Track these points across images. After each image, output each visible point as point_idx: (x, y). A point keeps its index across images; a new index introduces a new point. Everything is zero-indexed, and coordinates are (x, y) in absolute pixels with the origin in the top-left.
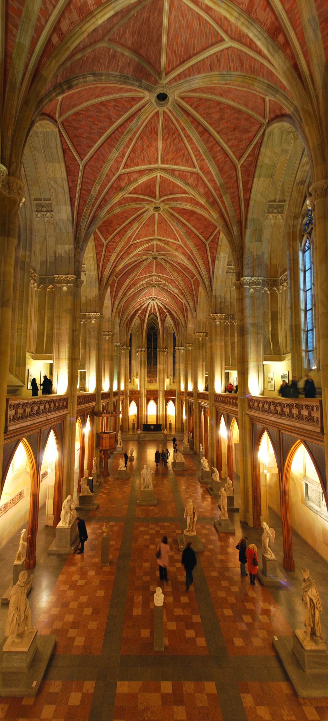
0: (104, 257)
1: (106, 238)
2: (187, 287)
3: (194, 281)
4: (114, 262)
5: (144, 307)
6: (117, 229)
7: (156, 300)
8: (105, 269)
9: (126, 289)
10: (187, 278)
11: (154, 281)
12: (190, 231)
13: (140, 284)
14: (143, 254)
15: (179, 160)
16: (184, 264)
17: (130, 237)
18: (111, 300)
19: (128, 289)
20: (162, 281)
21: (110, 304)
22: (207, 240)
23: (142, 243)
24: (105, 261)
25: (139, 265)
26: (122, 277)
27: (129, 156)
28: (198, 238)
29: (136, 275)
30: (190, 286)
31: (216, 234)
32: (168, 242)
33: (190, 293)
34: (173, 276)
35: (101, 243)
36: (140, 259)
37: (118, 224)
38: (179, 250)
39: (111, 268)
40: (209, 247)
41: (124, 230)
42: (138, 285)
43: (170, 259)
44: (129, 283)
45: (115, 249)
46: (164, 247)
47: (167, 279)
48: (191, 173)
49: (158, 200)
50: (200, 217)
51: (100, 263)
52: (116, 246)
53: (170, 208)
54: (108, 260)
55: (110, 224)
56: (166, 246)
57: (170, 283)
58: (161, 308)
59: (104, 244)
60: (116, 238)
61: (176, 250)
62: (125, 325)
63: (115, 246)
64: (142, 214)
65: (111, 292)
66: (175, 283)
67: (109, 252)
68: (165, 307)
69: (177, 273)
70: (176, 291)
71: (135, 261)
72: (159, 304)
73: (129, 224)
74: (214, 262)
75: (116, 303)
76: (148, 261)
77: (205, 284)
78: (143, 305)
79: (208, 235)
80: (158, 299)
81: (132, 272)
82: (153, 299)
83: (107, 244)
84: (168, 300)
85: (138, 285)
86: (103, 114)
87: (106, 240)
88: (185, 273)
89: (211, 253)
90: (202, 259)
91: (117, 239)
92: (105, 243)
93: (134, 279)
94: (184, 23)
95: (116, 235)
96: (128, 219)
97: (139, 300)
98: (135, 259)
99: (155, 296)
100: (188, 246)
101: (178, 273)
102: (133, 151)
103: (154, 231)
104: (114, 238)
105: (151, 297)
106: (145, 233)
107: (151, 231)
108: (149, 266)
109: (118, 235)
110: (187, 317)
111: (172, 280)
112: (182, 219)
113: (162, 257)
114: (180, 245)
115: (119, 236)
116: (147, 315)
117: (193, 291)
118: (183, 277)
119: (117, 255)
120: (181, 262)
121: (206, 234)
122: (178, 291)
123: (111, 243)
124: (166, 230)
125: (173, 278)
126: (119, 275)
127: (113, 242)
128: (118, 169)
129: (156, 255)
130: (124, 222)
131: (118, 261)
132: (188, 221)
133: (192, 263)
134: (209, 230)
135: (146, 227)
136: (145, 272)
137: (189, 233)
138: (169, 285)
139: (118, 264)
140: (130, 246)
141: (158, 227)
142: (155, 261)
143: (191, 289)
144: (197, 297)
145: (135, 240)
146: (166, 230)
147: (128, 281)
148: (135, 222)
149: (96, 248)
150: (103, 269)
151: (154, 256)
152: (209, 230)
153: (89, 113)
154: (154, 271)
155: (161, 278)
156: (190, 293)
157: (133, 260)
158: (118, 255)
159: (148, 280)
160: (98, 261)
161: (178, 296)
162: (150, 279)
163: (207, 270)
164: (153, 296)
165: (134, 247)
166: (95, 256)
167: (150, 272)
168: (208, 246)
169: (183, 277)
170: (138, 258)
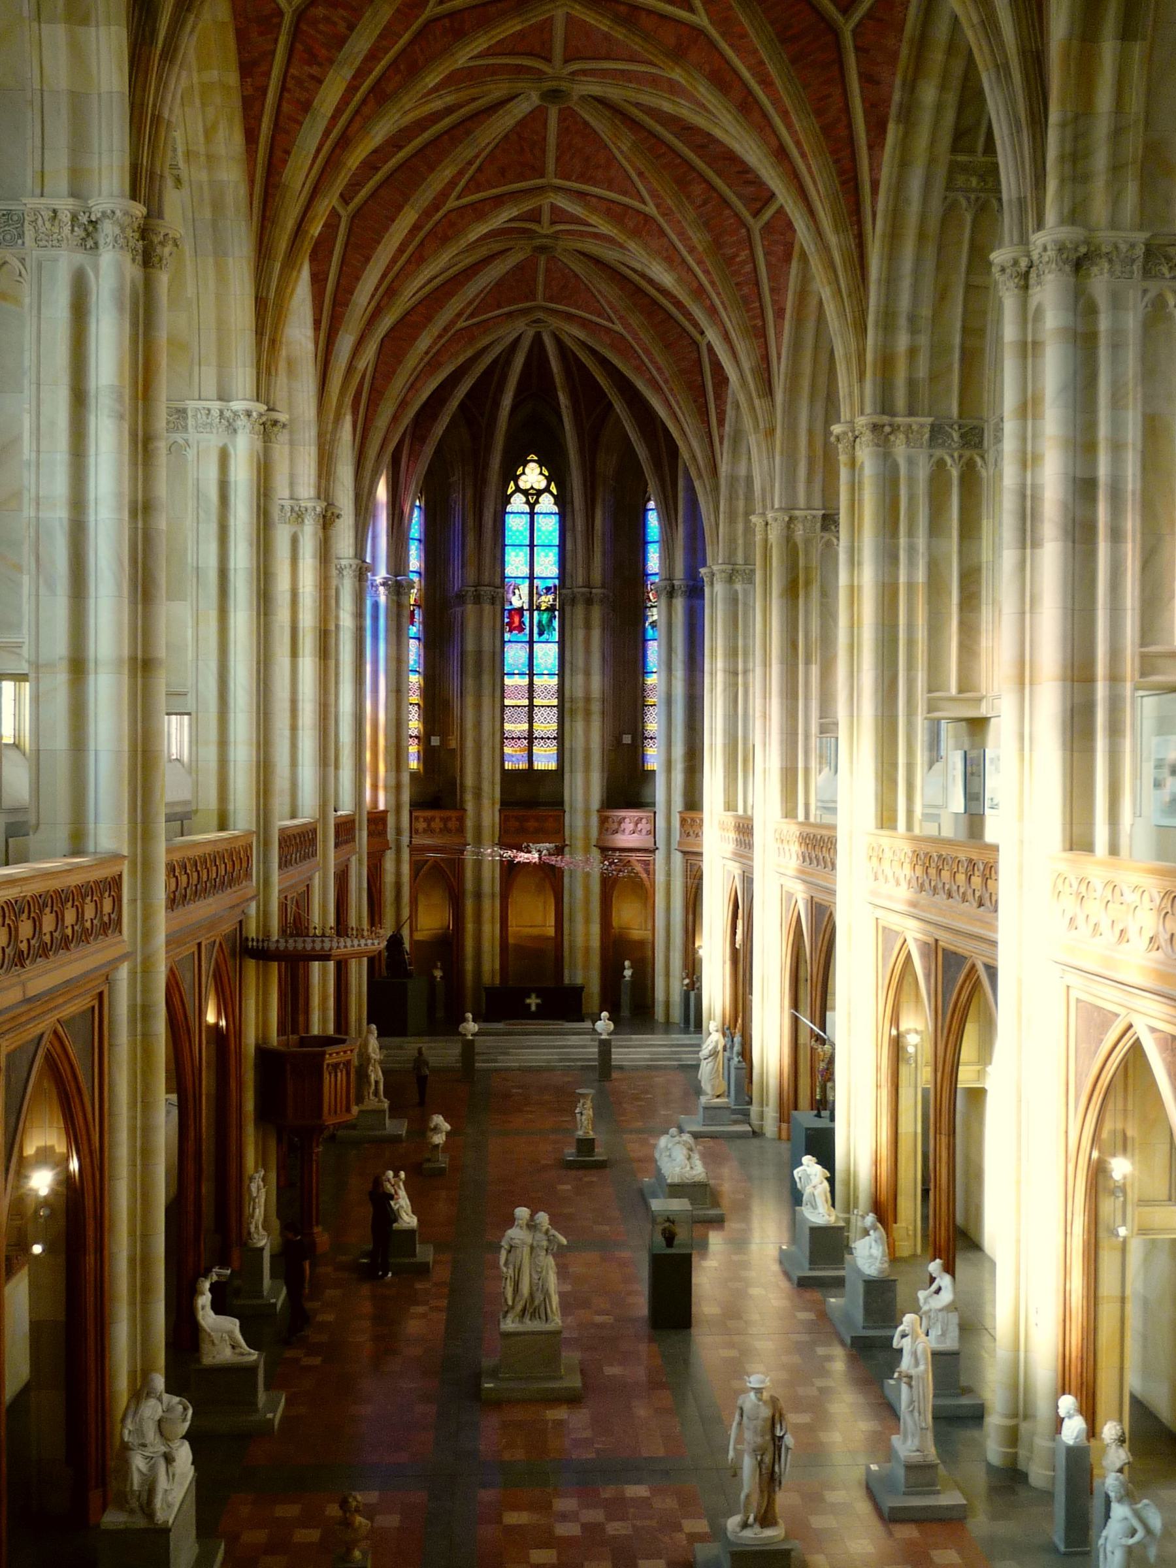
0: (284, 88)
2: (730, 260)
3: (768, 228)
4: (334, 118)
5: (488, 360)
7: (555, 323)
8: (288, 153)
9: (394, 261)
10: (727, 212)
11: (546, 217)
13: (472, 236)
14: (493, 71)
16: (718, 133)
18: (317, 323)
19: (408, 261)
20: (593, 219)
21: (310, 346)
22: (845, 11)
24: (286, 107)
26: (373, 194)
29: (452, 183)
30: (744, 255)
33: (746, 290)
34: (654, 195)
36: (474, 100)
39: (318, 150)
40: (857, 49)
42: (463, 243)
43: (637, 105)
44: (416, 228)
45: (341, 41)
46: (607, 37)
51: (259, 119)
52: (351, 28)
54: (306, 106)
56: (619, 34)
57: (635, 233)
58: (582, 367)
59: (280, 13)
61: (678, 54)
62: (387, 458)
63: (342, 27)
65: (318, 280)
66: (662, 233)
67: (312, 58)
68: (604, 362)
70: (667, 279)
71: (449, 110)
72: (569, 343)
74: (878, 129)
75: (346, 343)
76: (520, 109)
77: (826, 249)
78: (485, 349)
80: (569, 317)
81: (431, 169)
82: (541, 315)
84: (618, 327)
85: (463, 243)
88: (718, 182)
89: (868, 79)
90: (819, 113)
93: (437, 209)
97: (461, 324)
98: (450, 99)
99: (551, 299)
100: (743, 36)
105: (528, 304)
110: (721, 422)
111: (647, 218)
113: (596, 89)
114: (699, 32)
116: (507, 401)
117: (757, 284)
118: (705, 203)
119: (354, 77)
120: (699, 121)
122: (679, 280)
125: (651, 209)
129: (560, 79)
131: (357, 112)
133: (761, 130)
136: (503, 172)
138: (632, 245)
139: (356, 125)
140: (426, 25)
142: (553, 113)
143: (748, 268)
144: (780, 313)
147: (408, 218)
149: (241, 37)
150: (279, 153)
151: (553, 84)
154: (551, 166)
155: (587, 206)
156: (746, 290)
157: (437, 105)
158: (360, 74)
159: (515, 212)
160: (250, 106)
161: (678, 304)
162: (527, 206)
163: (841, 173)
164: (540, 302)
166: (233, 78)
168: (848, 42)
169: (705, 203)
170: (463, 95)
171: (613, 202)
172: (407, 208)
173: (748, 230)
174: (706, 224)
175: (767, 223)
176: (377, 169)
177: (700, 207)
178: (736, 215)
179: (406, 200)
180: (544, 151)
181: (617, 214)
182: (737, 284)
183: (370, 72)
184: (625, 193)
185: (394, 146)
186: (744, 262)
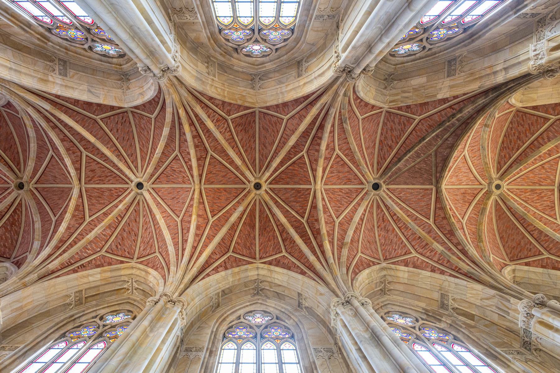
1: (233, 120)
3: (104, 256)
6: (237, 137)
10: (103, 243)
12: (236, 227)
15: (333, 204)
17: (223, 153)
23: (201, 168)
25: (120, 160)
27: (343, 160)
28: (231, 240)
31: (245, 260)
32: (203, 203)
35: (231, 113)
37: (242, 140)
38: (200, 219)
41: (234, 147)
47: (81, 208)
48: (331, 215)
49: (267, 187)
50: (252, 235)
52: (220, 132)
53: (255, 200)
55: (245, 130)
59: (229, 116)
60: (229, 133)
64: (249, 169)
69: (110, 225)
73: (239, 153)
79: (239, 251)
83: (226, 120)
86: (371, 143)
87: (231, 120)
91: (228, 134)
92: (229, 118)
94: (419, 197)
95: (232, 134)
96: (245, 152)
101: (109, 226)
102: (345, 163)
103: (212, 183)
104: (230, 131)
106: (215, 172)
107: (213, 180)
108: (107, 177)
109: (231, 136)
111: (84, 218)
112: (245, 216)
115: (230, 139)
117: (81, 260)
121: (239, 249)
123: (226, 126)
124: (219, 198)
126: (106, 125)
127: (226, 129)
128: (340, 150)
130: (243, 147)
131: (196, 130)
132: (244, 223)
134: (244, 251)
135: (224, 174)
136: (93, 171)
137: (233, 228)
139: (193, 129)
141: (218, 189)
143: (86, 255)
145: (212, 157)
146: (219, 198)
148: (241, 160)
152: (244, 251)
153: (374, 134)
165: (201, 157)
167: (88, 179)
171: (83, 206)
172: (95, 139)
173: (100, 251)
174: (96, 237)
175: (106, 256)
176: (111, 131)
177: (102, 234)
178: (104, 246)
179: (97, 139)
180: (98, 184)
181: (79, 208)
182: (77, 253)
183: (205, 135)
184: (89, 209)
185: (118, 138)
186: (86, 252)
